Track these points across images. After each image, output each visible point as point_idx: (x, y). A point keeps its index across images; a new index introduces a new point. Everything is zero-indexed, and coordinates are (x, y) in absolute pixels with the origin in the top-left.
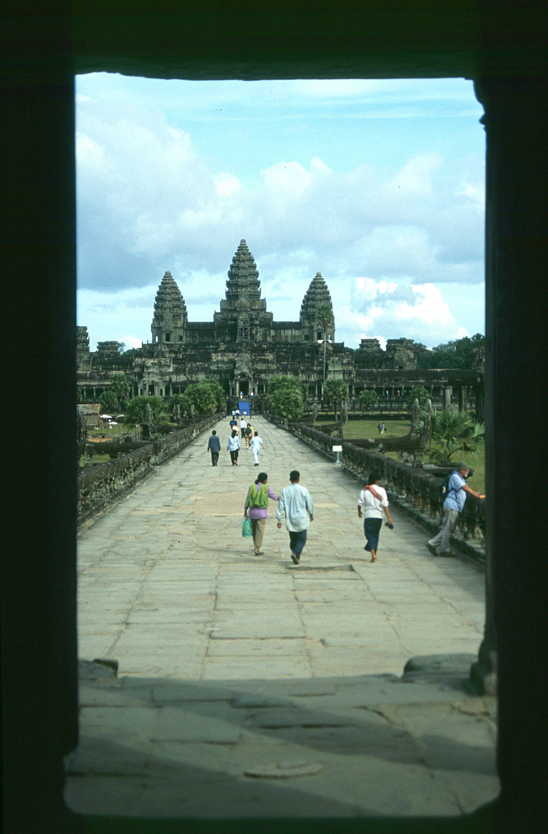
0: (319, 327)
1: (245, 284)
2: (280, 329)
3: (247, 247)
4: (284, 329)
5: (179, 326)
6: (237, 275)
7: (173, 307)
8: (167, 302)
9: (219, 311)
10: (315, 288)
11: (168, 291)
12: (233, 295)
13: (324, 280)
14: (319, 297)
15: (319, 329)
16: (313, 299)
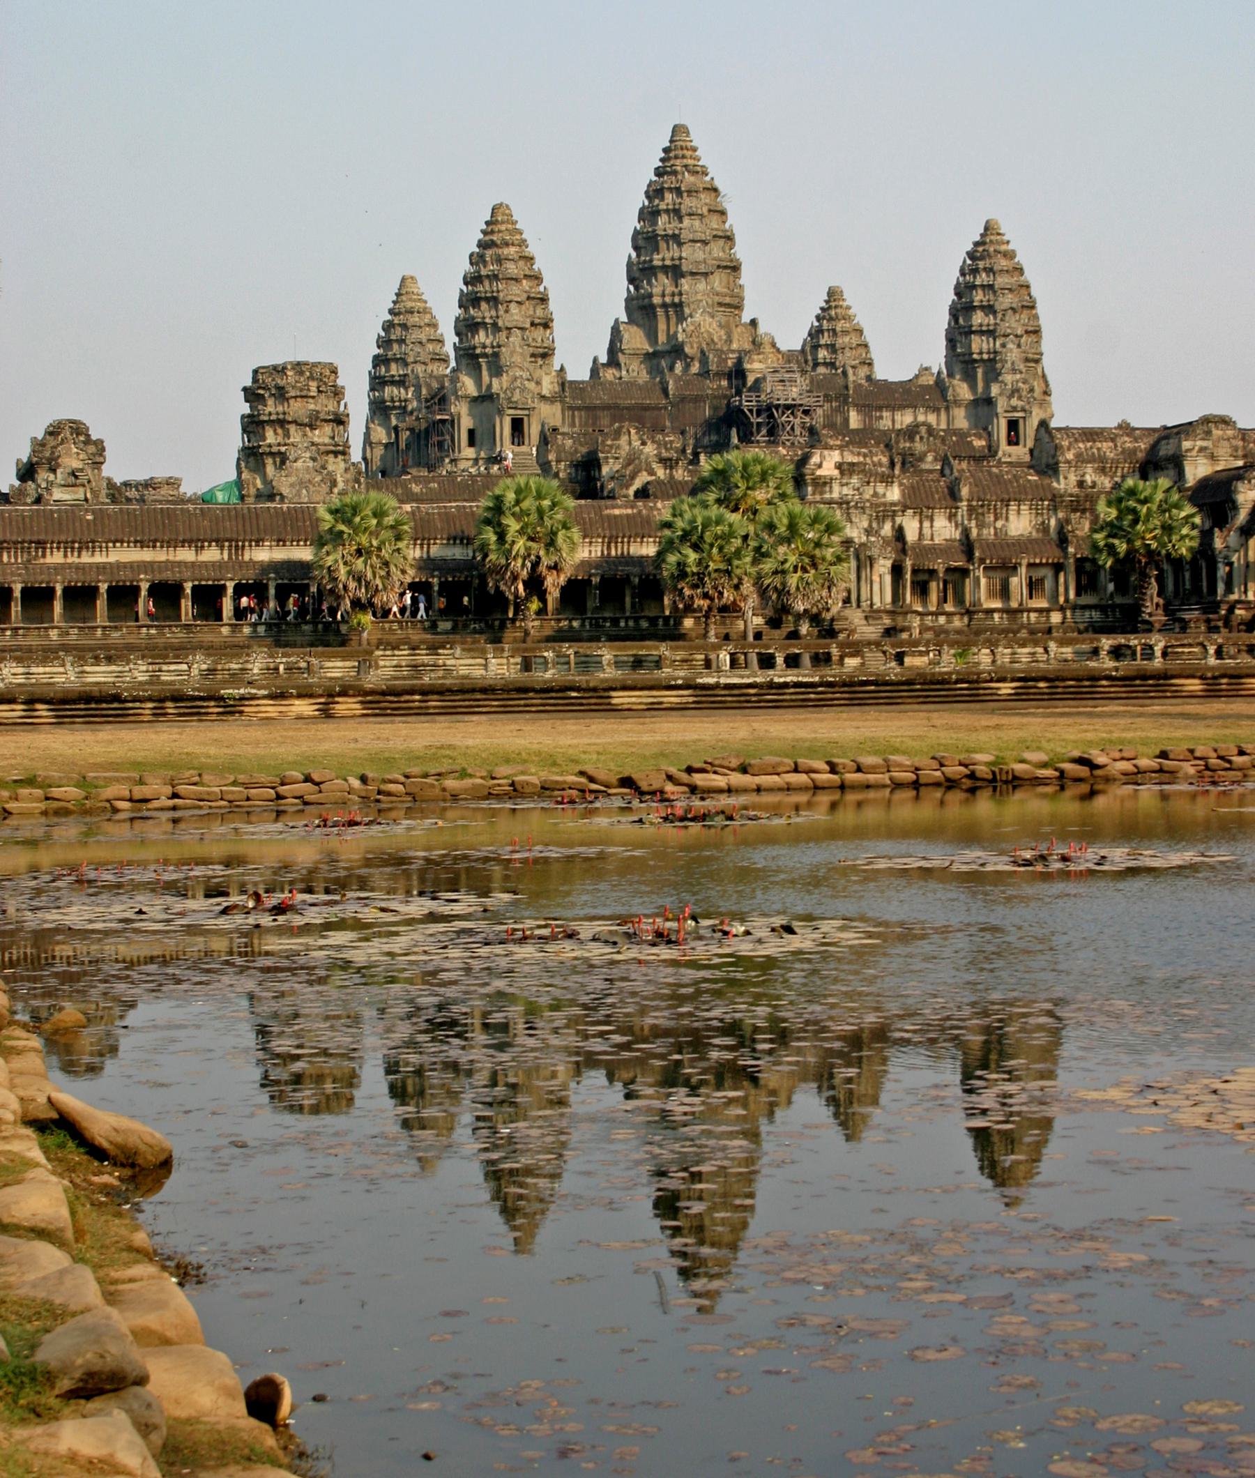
0: (1014, 402)
1: (702, 269)
2: (880, 408)
3: (695, 149)
4: (893, 409)
5: (545, 392)
6: (676, 238)
7: (532, 324)
8: (514, 308)
9: (603, 359)
10: (990, 270)
11: (512, 269)
12: (664, 305)
13: (1011, 247)
14: (1006, 301)
15: (1014, 409)
16: (989, 309)
